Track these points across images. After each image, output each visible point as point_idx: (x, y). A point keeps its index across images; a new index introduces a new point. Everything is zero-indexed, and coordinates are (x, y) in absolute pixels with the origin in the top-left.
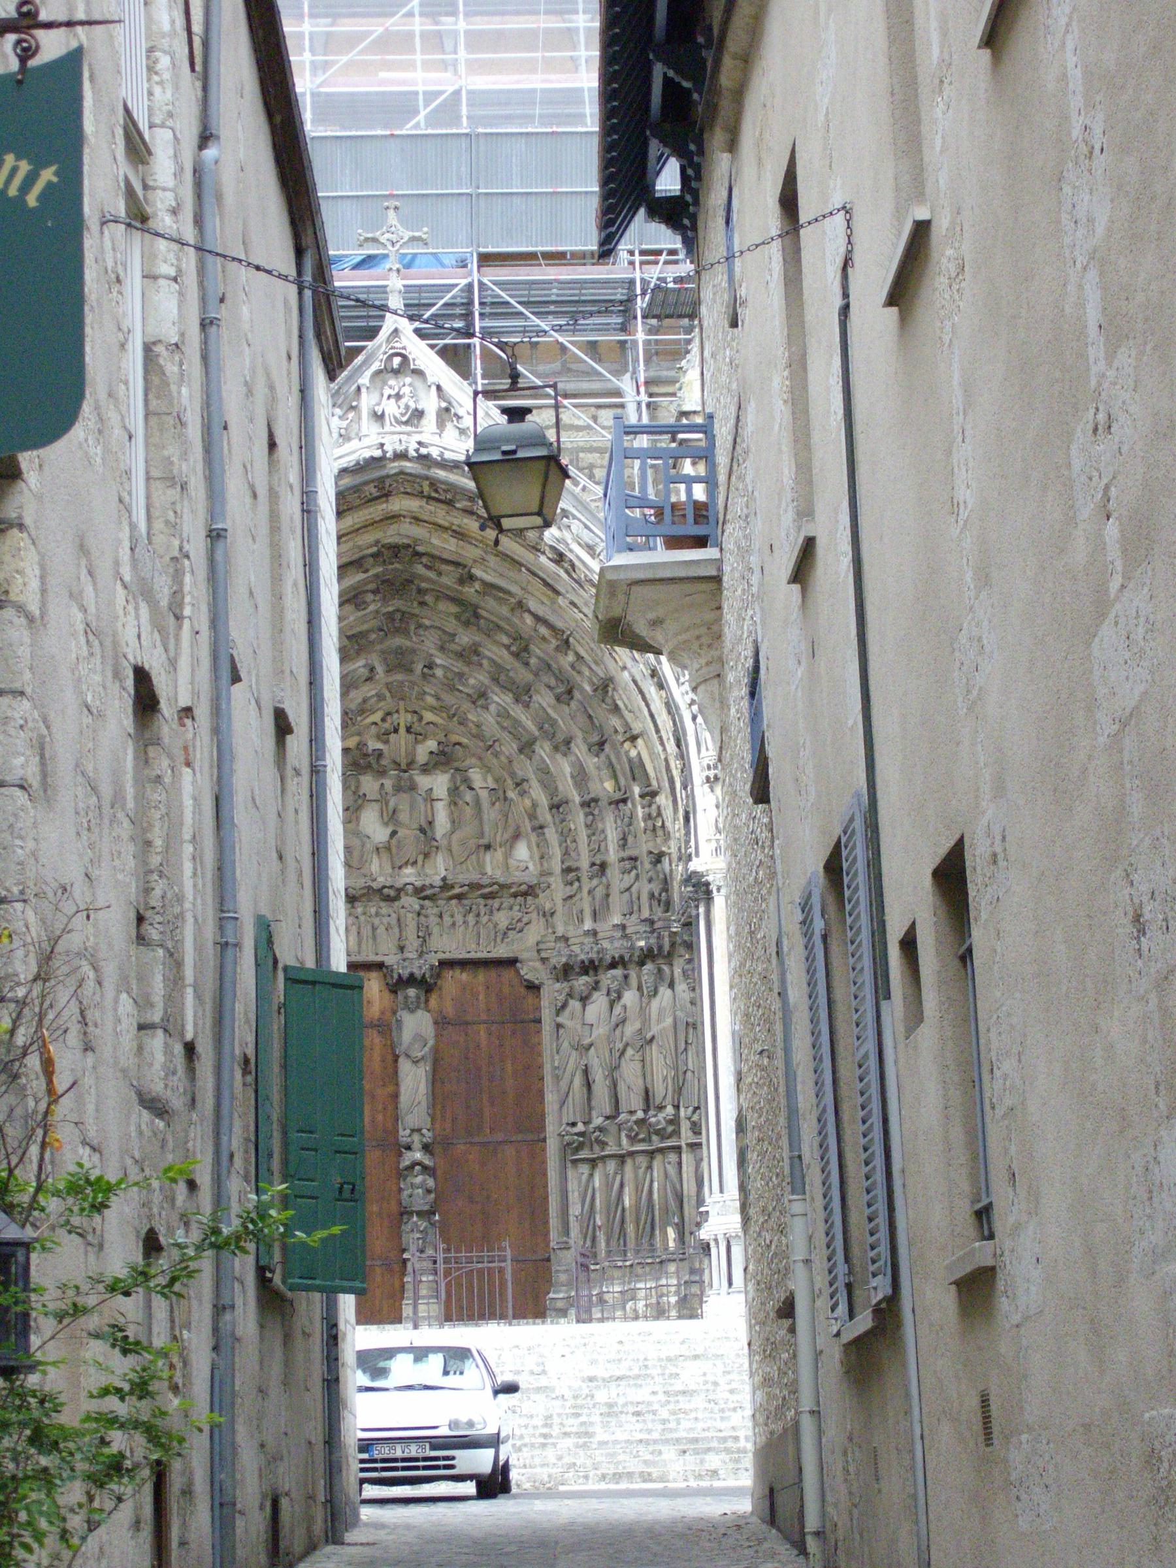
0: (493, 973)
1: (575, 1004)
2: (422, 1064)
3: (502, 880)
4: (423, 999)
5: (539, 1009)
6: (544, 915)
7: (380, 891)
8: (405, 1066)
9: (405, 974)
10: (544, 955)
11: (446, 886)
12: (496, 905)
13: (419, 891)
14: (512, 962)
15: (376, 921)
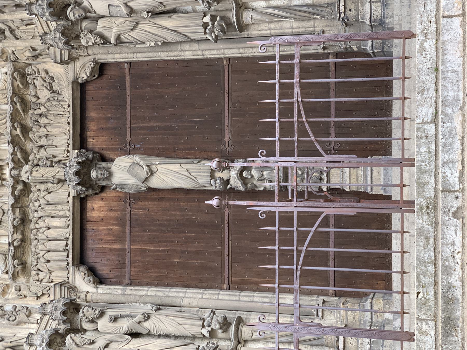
0: (90, 104)
1: (100, 26)
2: (154, 168)
3: (10, 94)
4: (104, 164)
5: (118, 64)
6: (36, 57)
7: (17, 199)
8: (155, 182)
9: (75, 180)
10: (66, 57)
11: (14, 142)
12: (34, 100)
13: (17, 165)
14: (81, 88)
15: (42, 201)
